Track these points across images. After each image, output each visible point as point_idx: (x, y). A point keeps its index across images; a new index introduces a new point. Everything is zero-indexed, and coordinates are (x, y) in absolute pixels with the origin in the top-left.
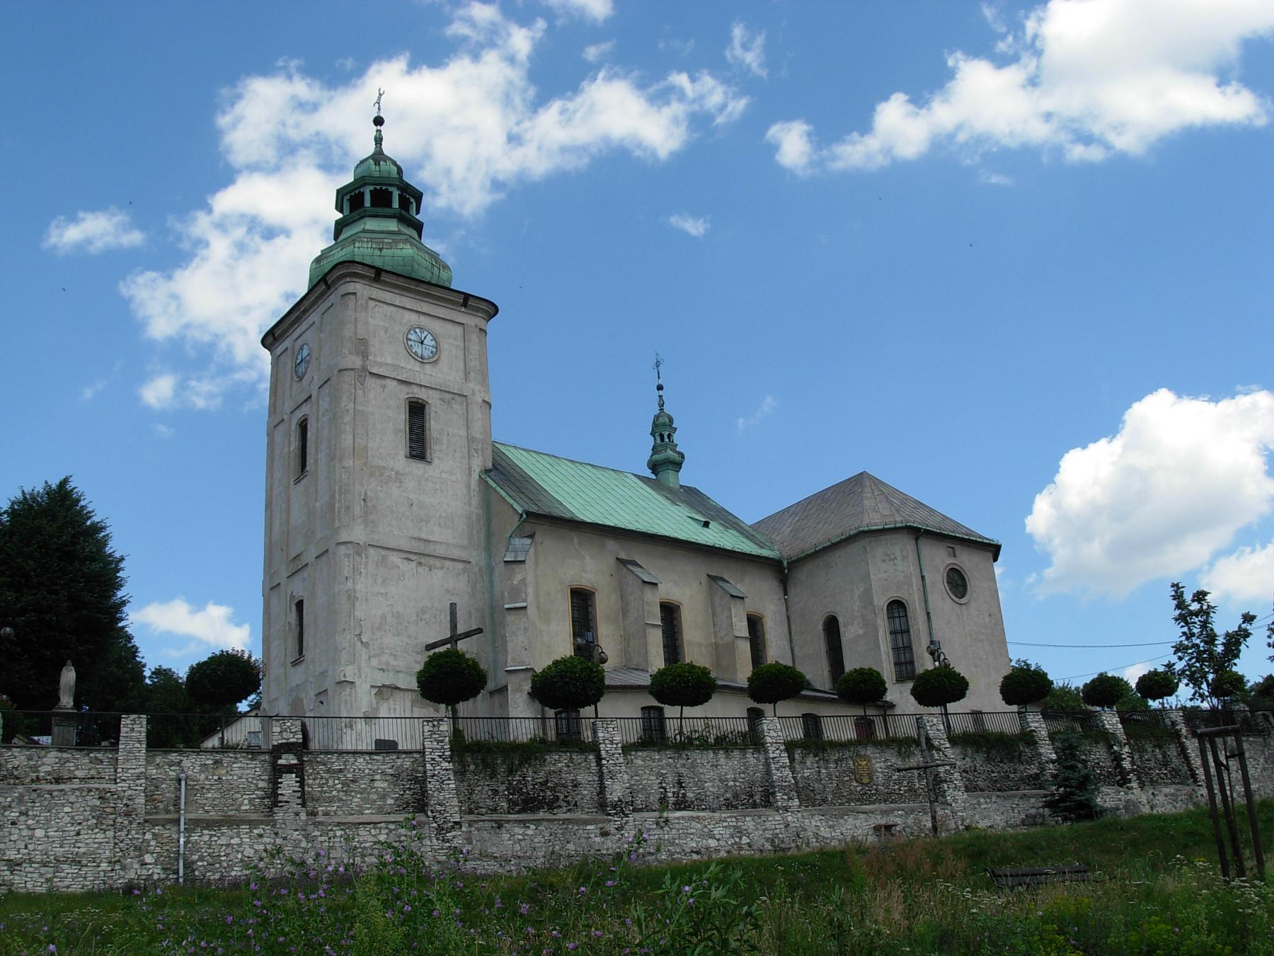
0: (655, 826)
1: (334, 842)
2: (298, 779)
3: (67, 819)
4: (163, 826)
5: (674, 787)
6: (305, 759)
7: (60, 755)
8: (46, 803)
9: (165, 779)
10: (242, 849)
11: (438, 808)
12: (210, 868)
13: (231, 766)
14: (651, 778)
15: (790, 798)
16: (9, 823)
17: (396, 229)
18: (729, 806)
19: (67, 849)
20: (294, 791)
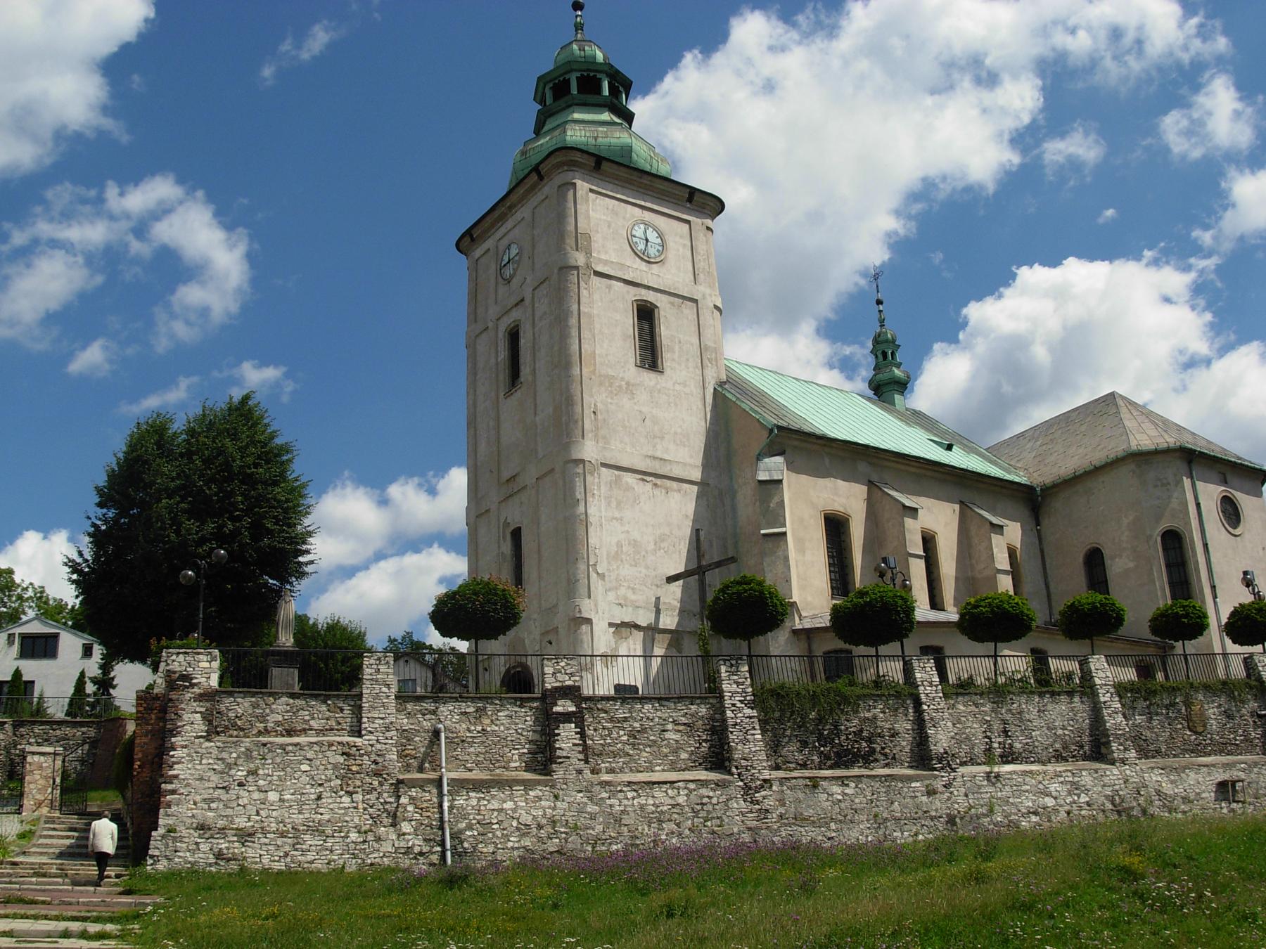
0: (985, 783)
1: (625, 806)
3: (305, 779)
4: (421, 787)
5: (999, 736)
6: (584, 706)
7: (291, 701)
8: (278, 760)
9: (419, 731)
11: (744, 763)
12: (481, 838)
13: (496, 714)
14: (975, 725)
15: (1125, 749)
16: (236, 784)
18: (1059, 758)
19: (307, 816)
20: (574, 745)
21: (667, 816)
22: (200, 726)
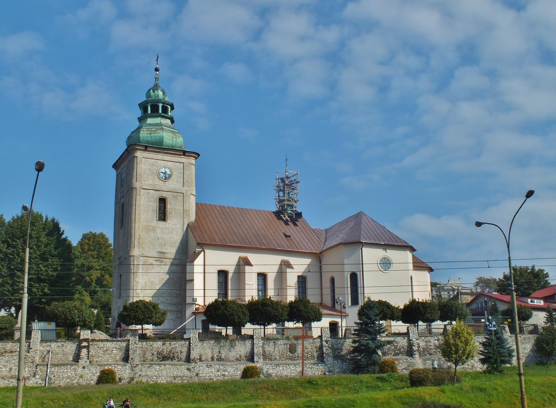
2: (87, 350)
10: (67, 373)
20: (86, 354)
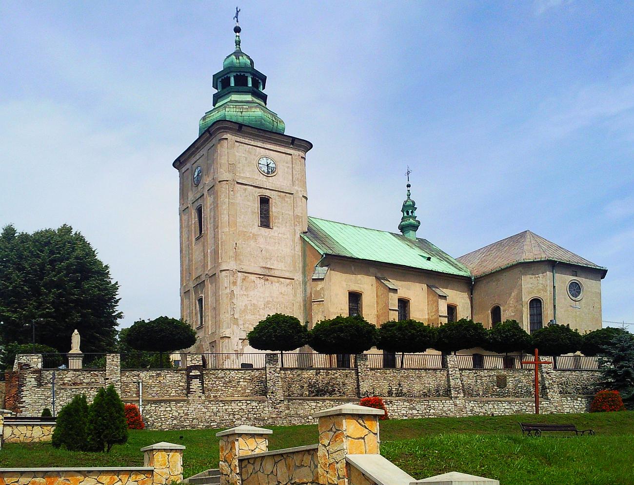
1: (219, 409)
9: (131, 383)
17: (251, 100)
20: (198, 387)
21: (237, 413)
22: (34, 382)
